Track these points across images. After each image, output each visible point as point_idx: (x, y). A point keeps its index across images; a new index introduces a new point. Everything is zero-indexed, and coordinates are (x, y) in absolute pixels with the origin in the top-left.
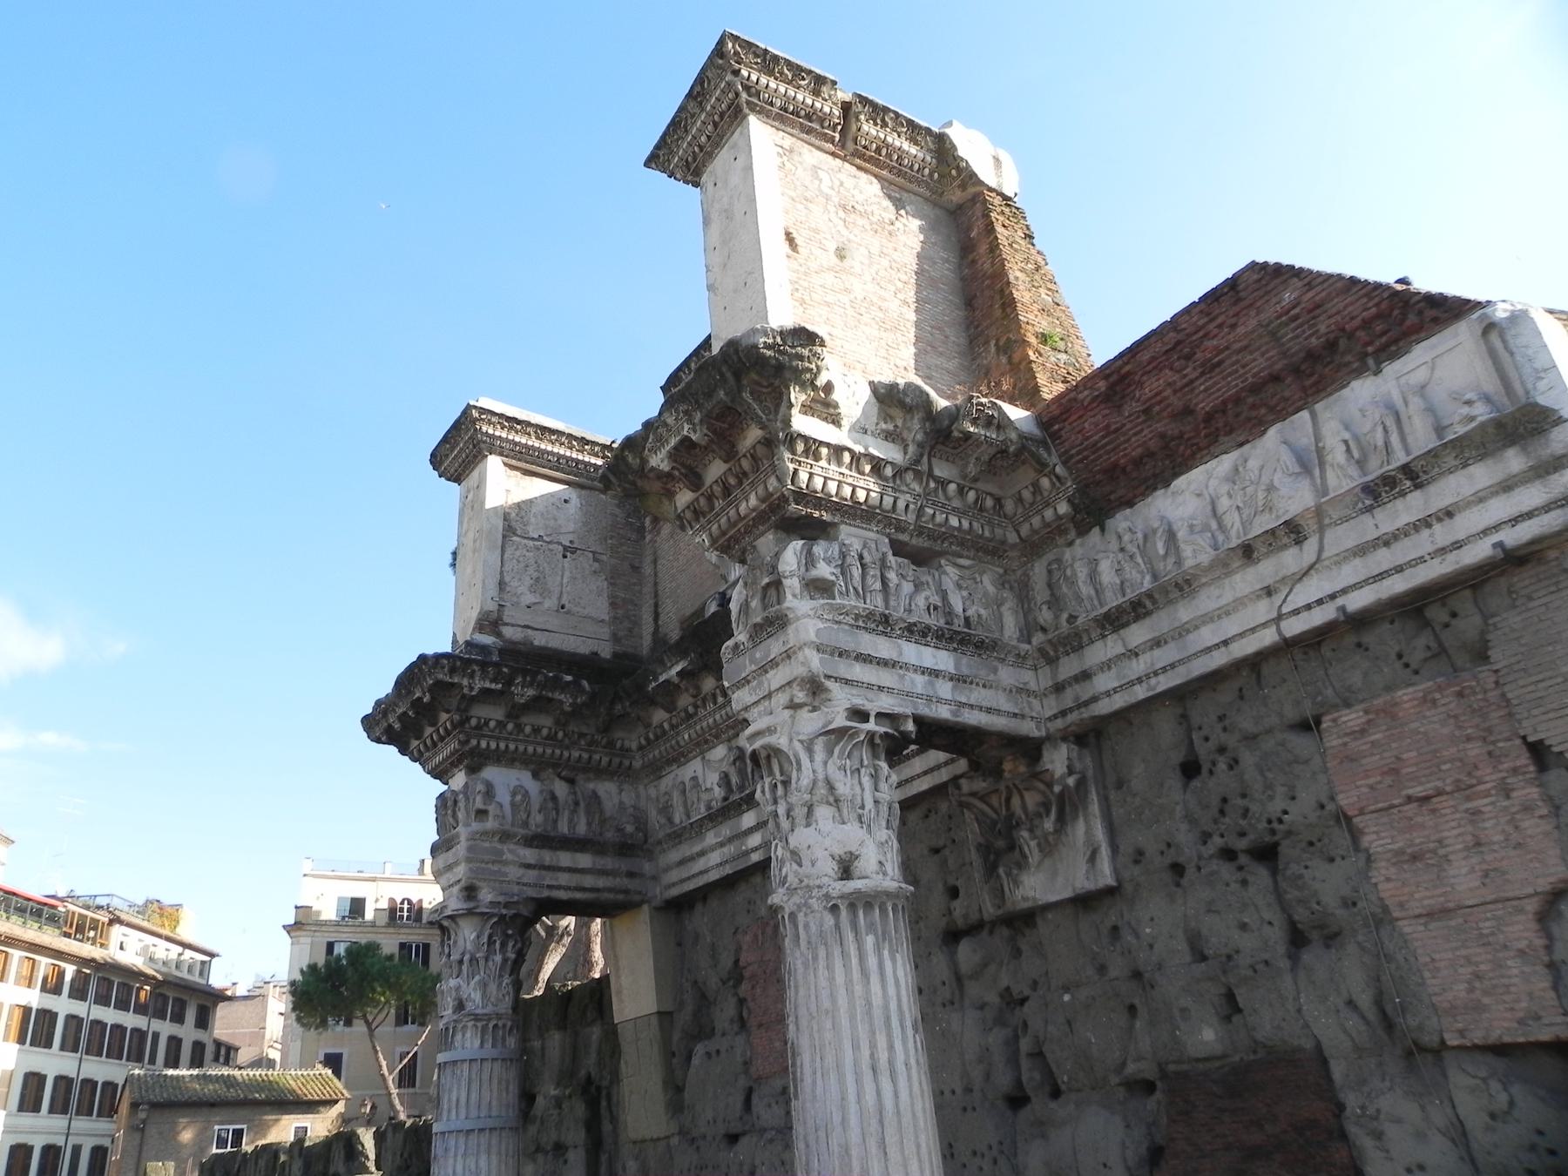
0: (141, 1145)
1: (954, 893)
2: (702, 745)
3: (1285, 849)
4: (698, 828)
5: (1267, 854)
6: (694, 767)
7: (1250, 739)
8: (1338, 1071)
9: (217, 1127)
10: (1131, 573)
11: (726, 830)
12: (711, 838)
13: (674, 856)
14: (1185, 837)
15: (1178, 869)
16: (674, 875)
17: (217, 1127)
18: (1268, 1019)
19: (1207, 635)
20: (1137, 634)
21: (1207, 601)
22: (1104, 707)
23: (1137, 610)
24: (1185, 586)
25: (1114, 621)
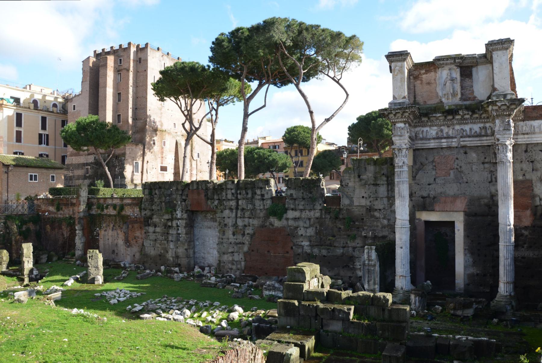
0: (8, 178)
1: (485, 158)
2: (430, 126)
3: (535, 162)
4: (429, 139)
5: (532, 162)
6: (428, 129)
7: (535, 151)
8: (533, 182)
9: (29, 174)
10: (527, 129)
11: (437, 141)
12: (432, 141)
13: (420, 142)
14: (524, 158)
15: (521, 162)
16: (420, 145)
17: (29, 174)
18: (528, 177)
19: (535, 139)
20: (526, 136)
21: (536, 136)
22: (518, 143)
23: (527, 134)
24: (534, 133)
25: (524, 134)
